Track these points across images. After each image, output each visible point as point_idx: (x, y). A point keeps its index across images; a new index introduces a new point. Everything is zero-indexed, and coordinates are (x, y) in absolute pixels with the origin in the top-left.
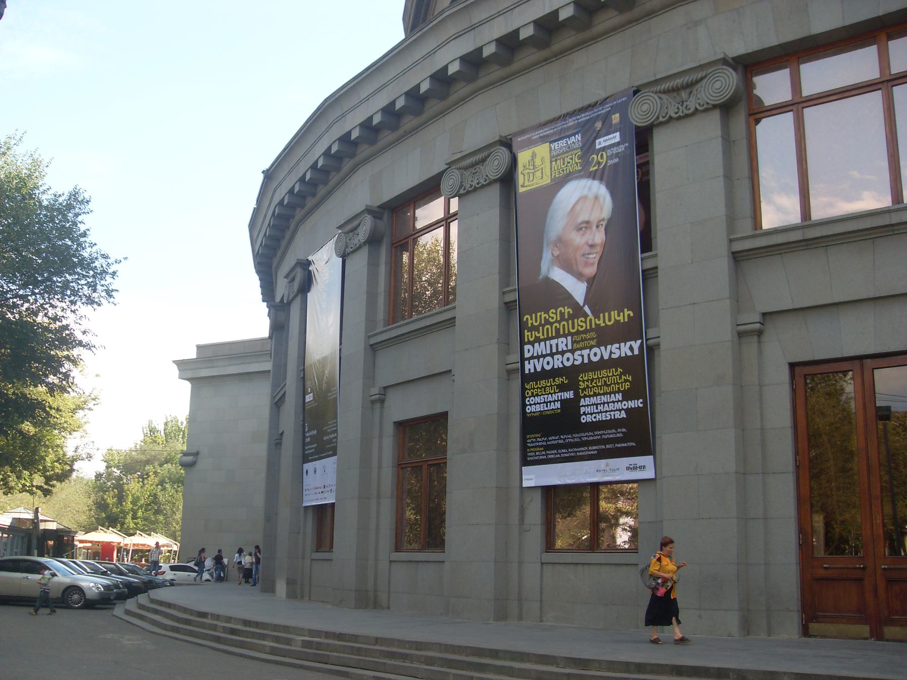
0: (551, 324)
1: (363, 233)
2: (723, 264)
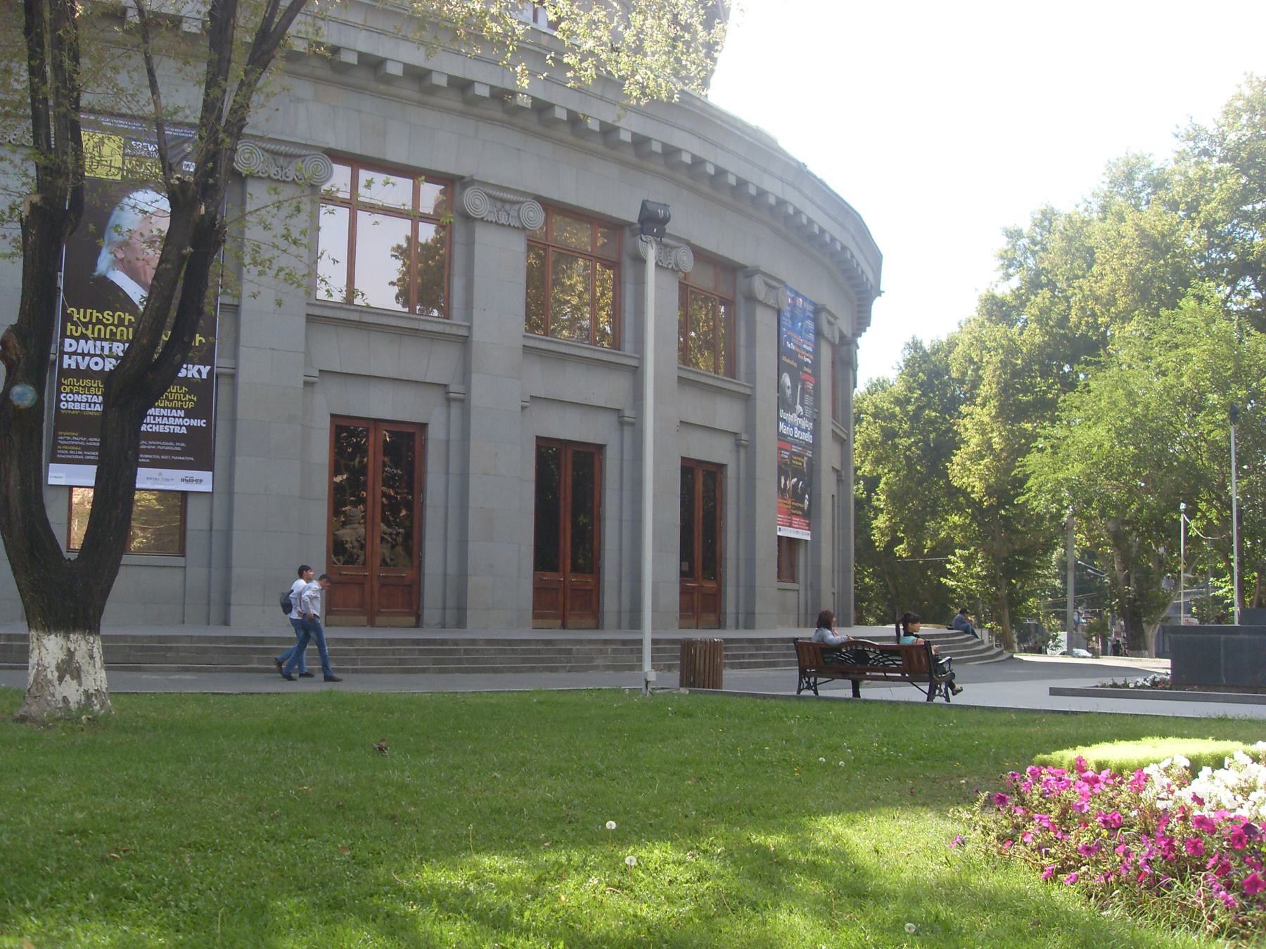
0: (106, 326)
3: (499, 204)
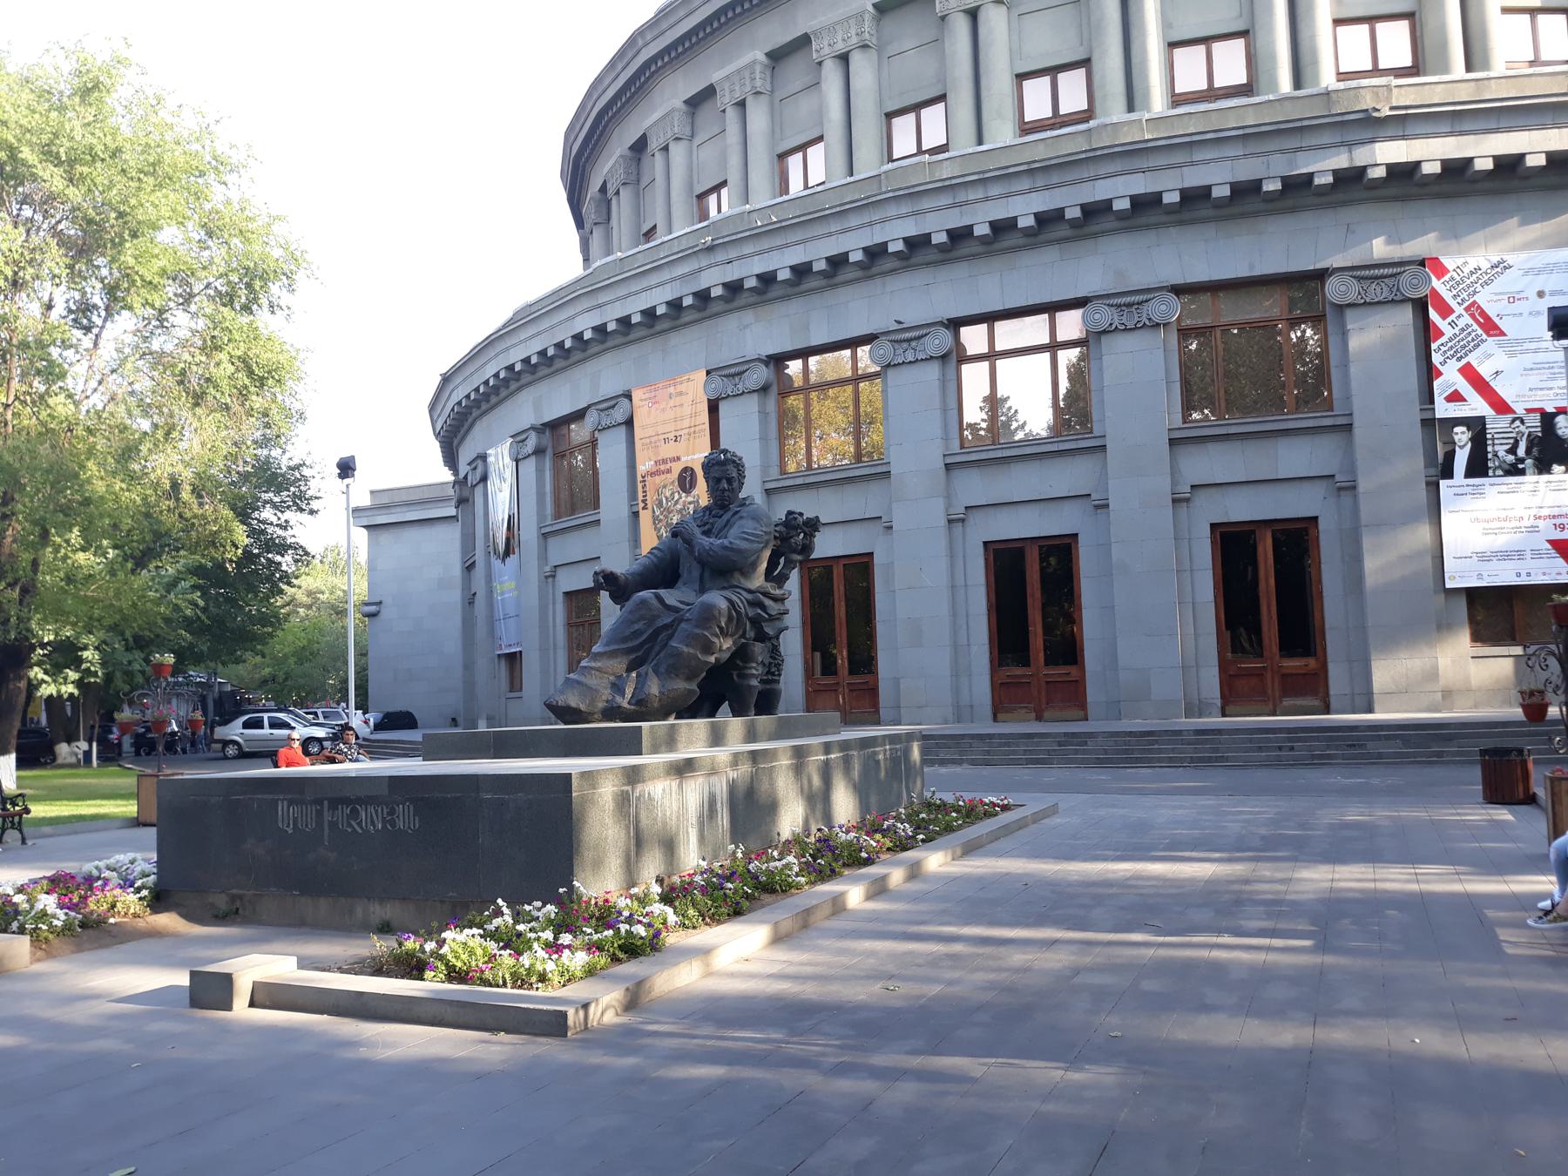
1: (532, 442)
3: (905, 345)
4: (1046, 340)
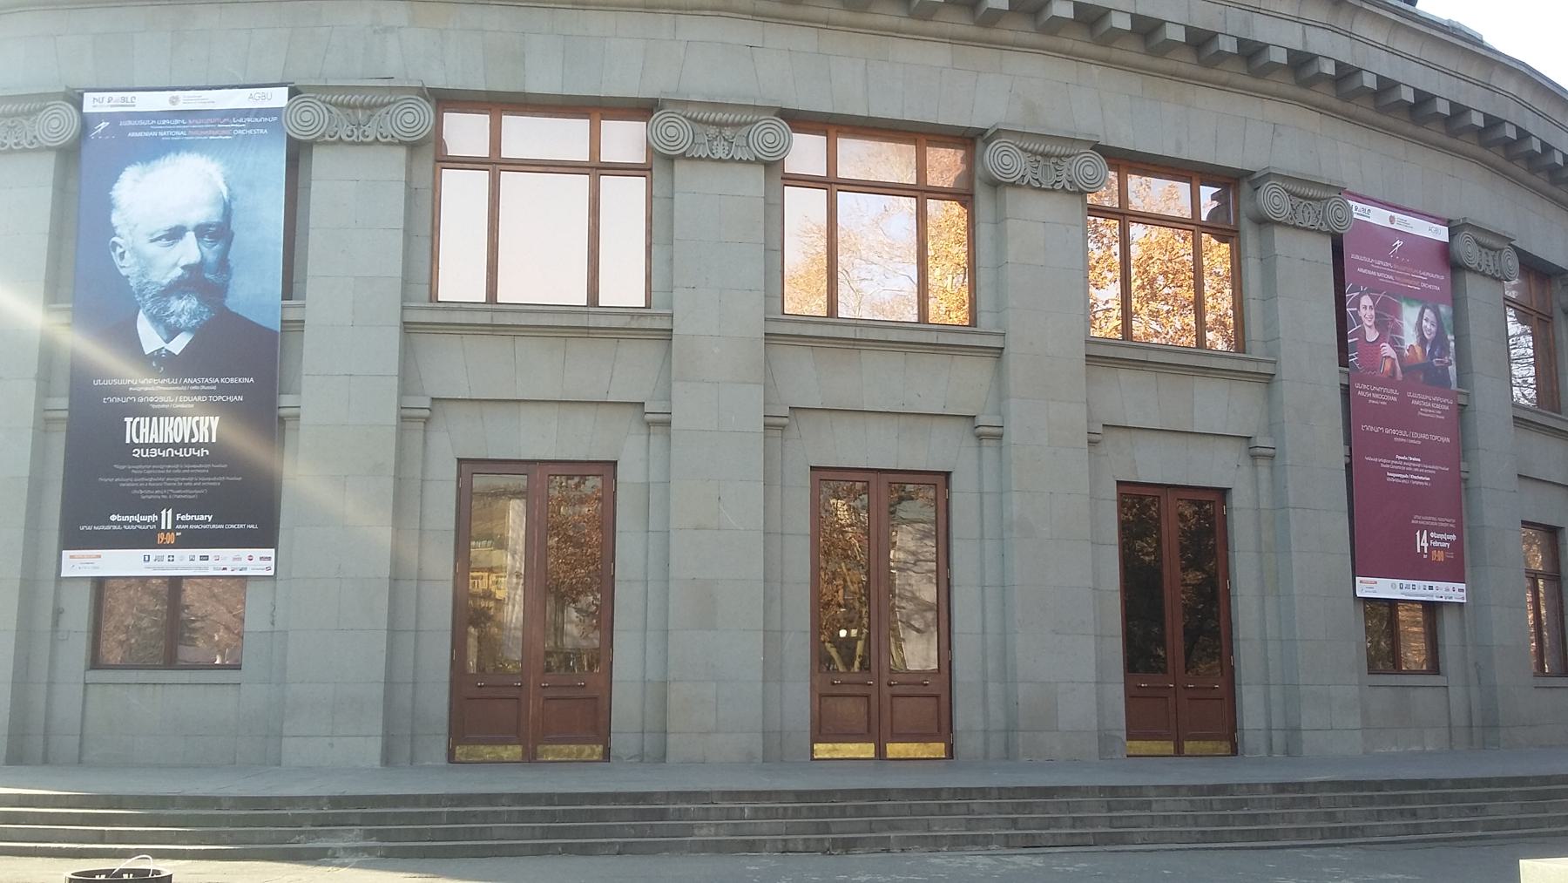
2: (394, 334)
3: (713, 131)
4: (910, 178)
